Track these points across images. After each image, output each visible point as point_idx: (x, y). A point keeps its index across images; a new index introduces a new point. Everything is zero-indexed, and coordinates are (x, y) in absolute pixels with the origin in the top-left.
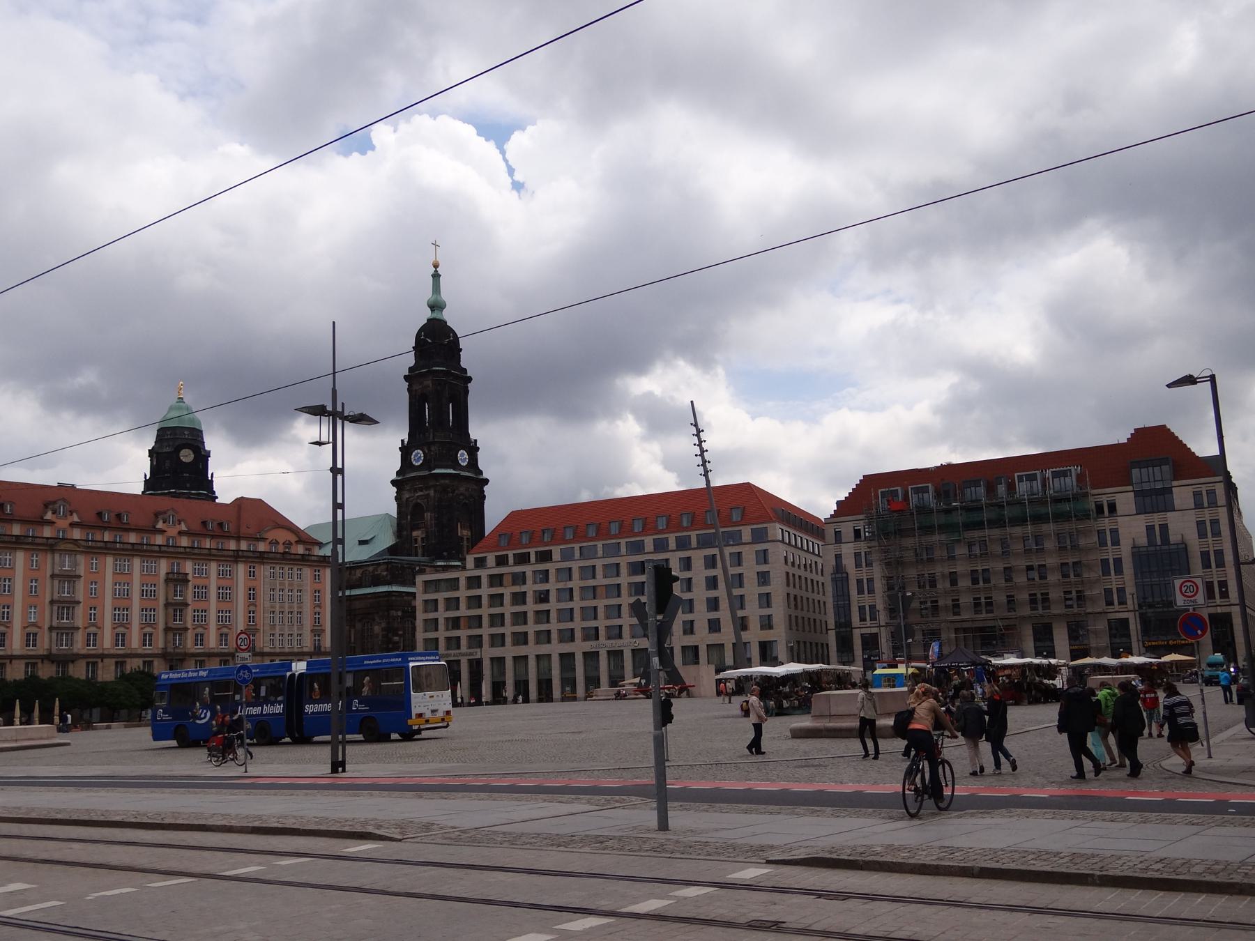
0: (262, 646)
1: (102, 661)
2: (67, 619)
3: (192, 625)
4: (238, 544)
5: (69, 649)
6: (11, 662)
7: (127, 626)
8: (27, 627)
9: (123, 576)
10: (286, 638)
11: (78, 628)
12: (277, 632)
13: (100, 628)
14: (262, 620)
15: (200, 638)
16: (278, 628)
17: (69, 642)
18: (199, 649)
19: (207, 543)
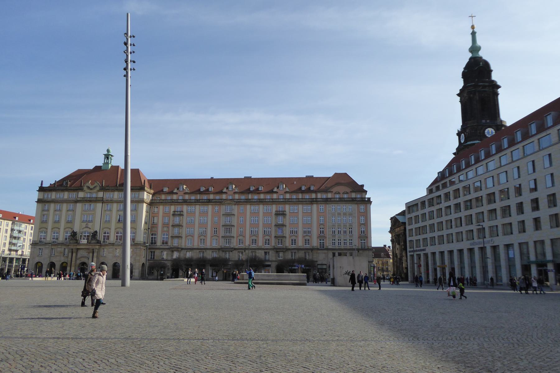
0: (327, 245)
1: (245, 251)
2: (229, 233)
3: (289, 235)
4: (317, 196)
5: (230, 246)
6: (206, 251)
7: (257, 236)
8: (213, 237)
9: (255, 214)
10: (342, 242)
11: (233, 237)
12: (337, 238)
13: (244, 237)
14: (328, 233)
15: (294, 242)
16: (337, 237)
17: (230, 243)
18: (294, 246)
19: (300, 196)
